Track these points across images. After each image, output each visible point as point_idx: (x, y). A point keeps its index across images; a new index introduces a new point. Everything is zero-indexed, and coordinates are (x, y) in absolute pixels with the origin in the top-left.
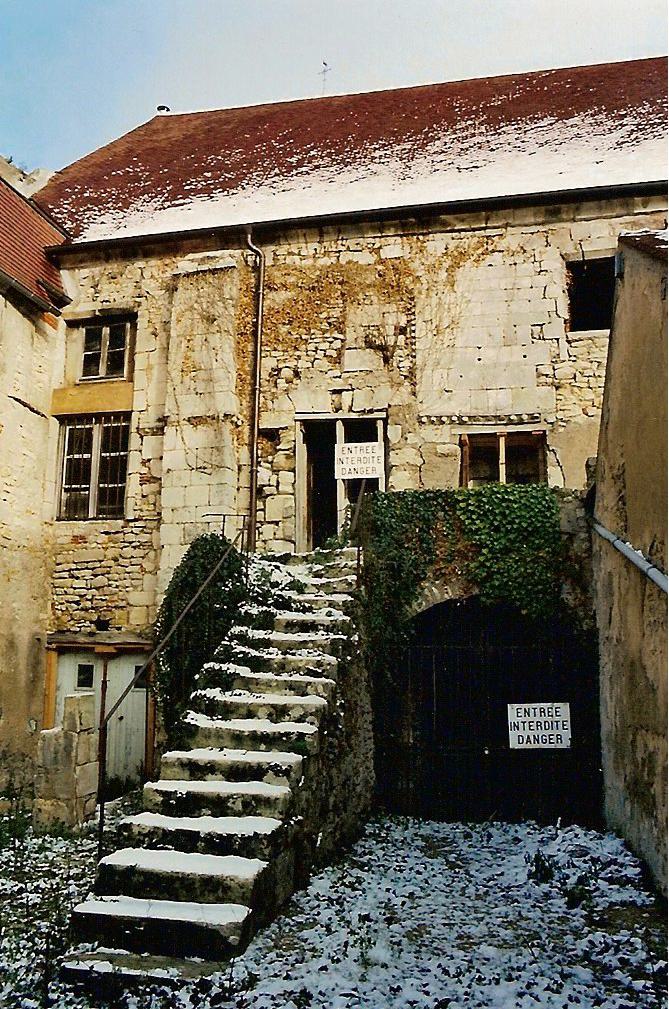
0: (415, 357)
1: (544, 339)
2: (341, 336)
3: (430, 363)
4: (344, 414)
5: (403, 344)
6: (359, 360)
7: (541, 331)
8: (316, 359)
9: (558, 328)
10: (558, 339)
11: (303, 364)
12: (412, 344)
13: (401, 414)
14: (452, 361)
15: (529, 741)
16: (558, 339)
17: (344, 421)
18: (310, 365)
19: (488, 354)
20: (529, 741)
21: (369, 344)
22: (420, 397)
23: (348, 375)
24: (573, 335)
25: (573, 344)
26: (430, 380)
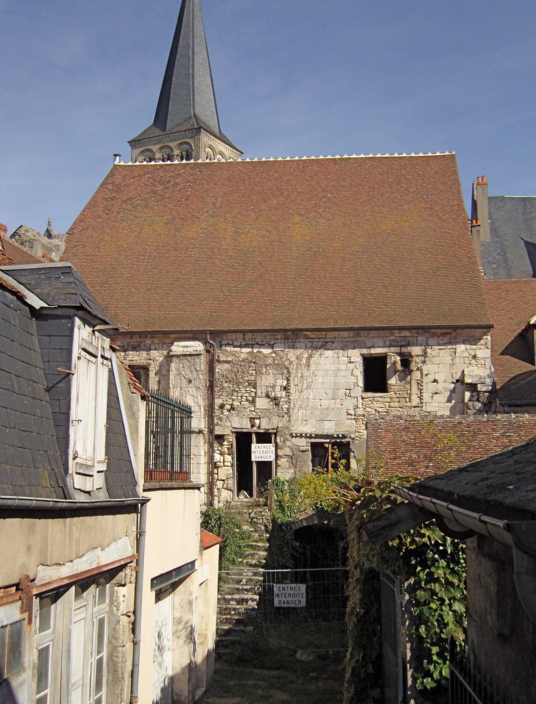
0: (290, 403)
1: (350, 397)
2: (255, 390)
3: (297, 406)
4: (255, 429)
5: (285, 396)
6: (262, 403)
7: (350, 393)
8: (242, 401)
9: (359, 391)
10: (357, 397)
11: (236, 403)
12: (288, 396)
13: (283, 431)
14: (307, 406)
15: (284, 603)
16: (357, 397)
17: (255, 433)
18: (239, 404)
19: (325, 403)
20: (284, 603)
21: (267, 396)
22: (292, 422)
23: (258, 410)
24: (365, 395)
25: (364, 400)
26: (298, 414)
